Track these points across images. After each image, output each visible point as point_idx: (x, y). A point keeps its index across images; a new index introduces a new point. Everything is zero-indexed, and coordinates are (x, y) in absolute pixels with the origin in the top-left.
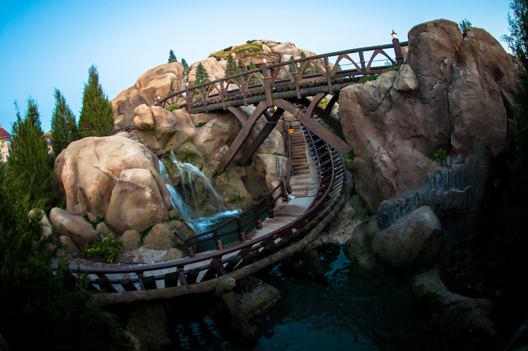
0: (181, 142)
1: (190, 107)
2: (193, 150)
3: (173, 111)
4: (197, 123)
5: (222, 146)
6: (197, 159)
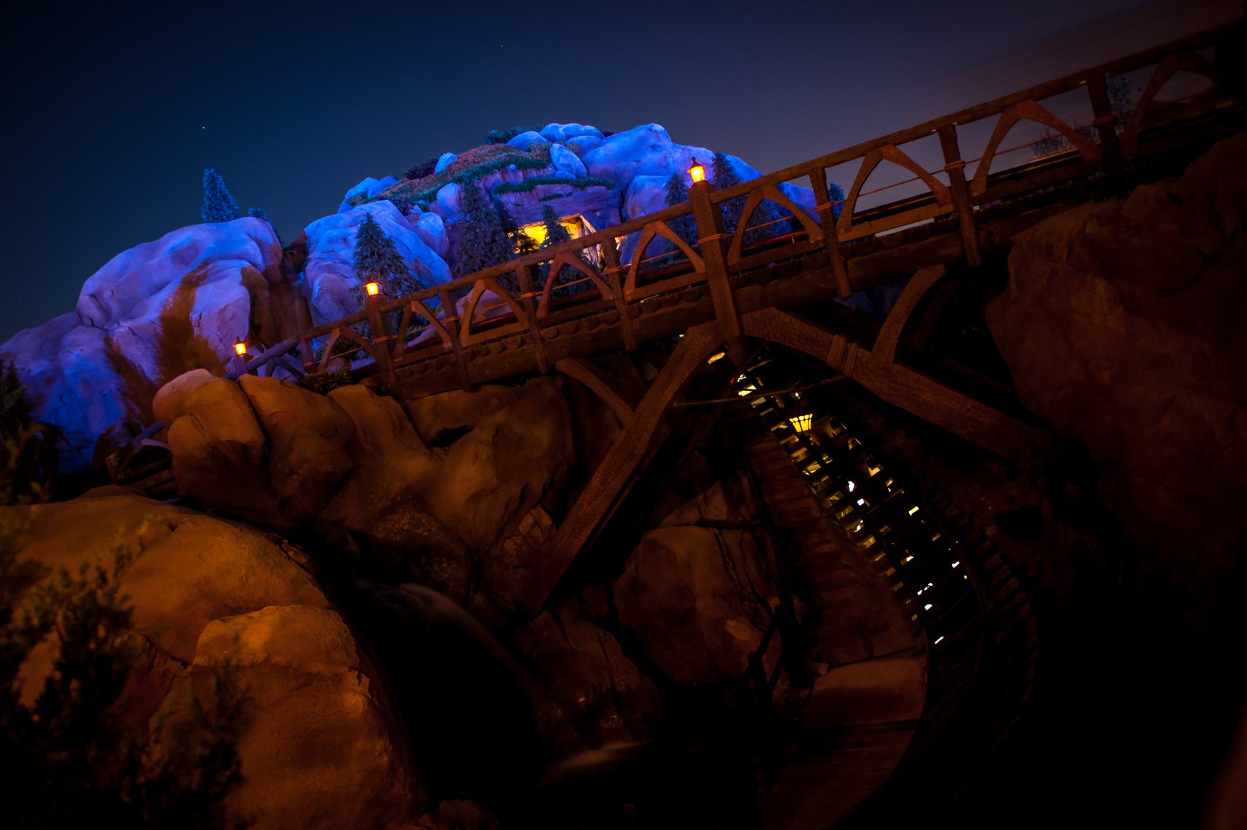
0: (379, 505)
1: (391, 373)
2: (430, 531)
3: (331, 393)
4: (433, 433)
5: (528, 512)
6: (444, 565)
